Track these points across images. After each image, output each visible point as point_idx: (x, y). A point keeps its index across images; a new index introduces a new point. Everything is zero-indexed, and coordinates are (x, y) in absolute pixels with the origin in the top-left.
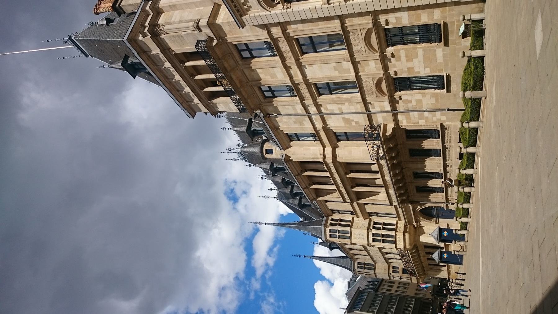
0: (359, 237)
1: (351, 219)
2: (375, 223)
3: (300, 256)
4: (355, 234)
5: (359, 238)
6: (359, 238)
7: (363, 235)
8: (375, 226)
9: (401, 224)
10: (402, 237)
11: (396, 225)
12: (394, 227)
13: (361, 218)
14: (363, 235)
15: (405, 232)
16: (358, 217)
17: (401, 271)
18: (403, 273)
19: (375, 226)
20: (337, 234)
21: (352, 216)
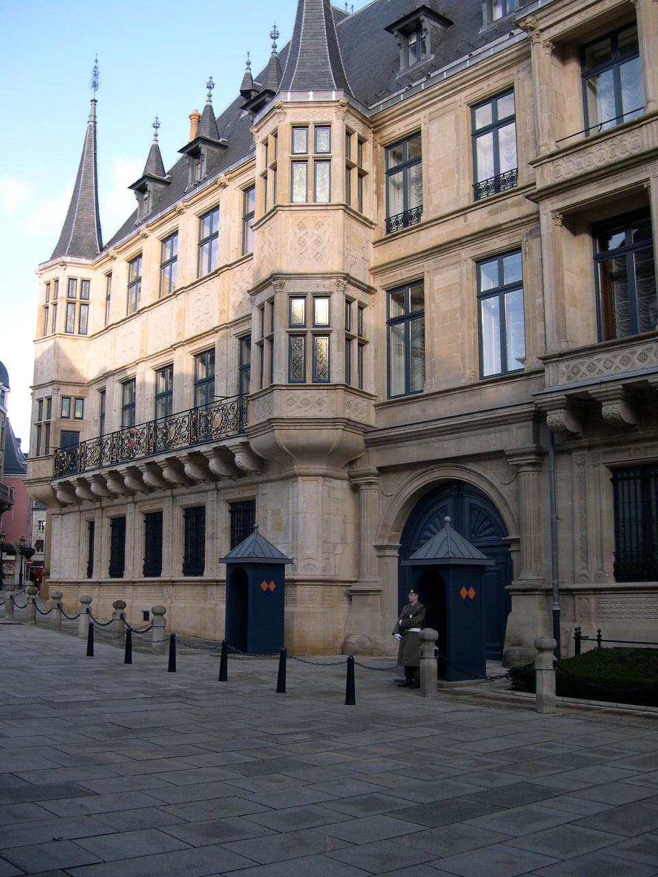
0: (310, 242)
1: (369, 213)
2: (361, 307)
3: (95, 85)
4: (319, 225)
5: (302, 242)
6: (302, 242)
7: (318, 256)
8: (355, 305)
9: (365, 413)
10: (325, 412)
11: (360, 393)
12: (354, 384)
13: (377, 257)
14: (318, 256)
15: (349, 424)
16: (377, 243)
17: (67, 426)
18: (65, 434)
19: (355, 305)
20: (311, 154)
21: (383, 224)
